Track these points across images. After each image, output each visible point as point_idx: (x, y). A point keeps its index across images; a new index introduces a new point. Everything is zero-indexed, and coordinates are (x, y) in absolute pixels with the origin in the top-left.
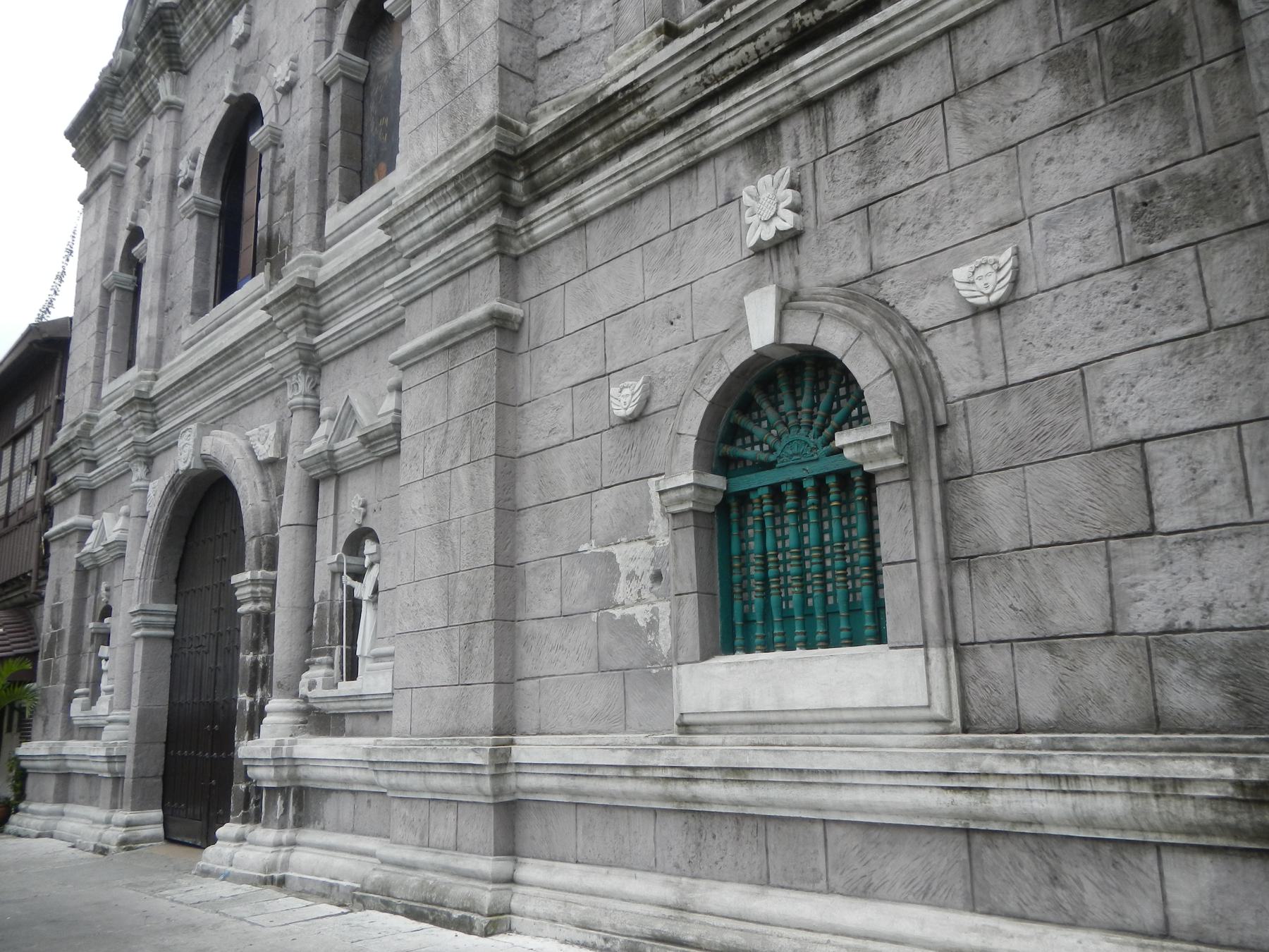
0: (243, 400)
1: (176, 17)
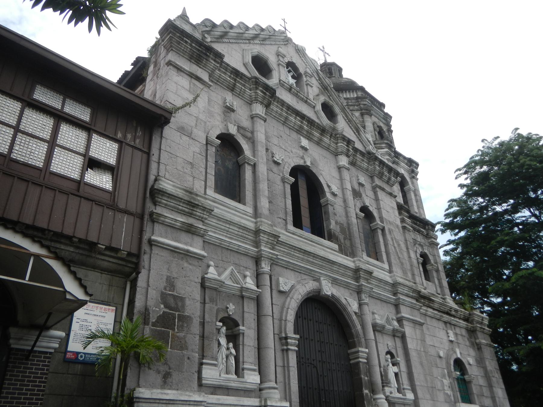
0: (337, 282)
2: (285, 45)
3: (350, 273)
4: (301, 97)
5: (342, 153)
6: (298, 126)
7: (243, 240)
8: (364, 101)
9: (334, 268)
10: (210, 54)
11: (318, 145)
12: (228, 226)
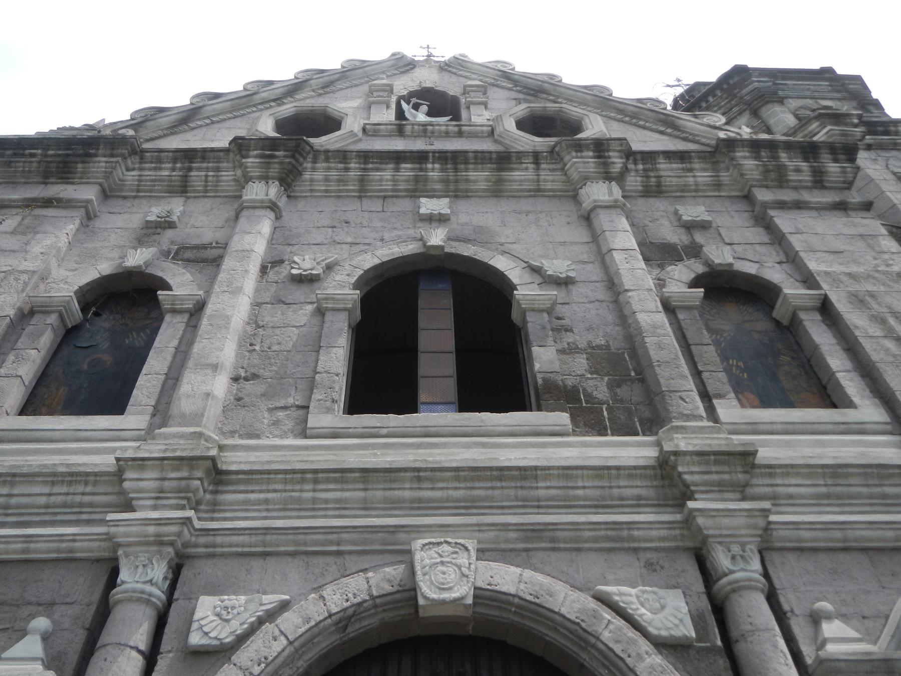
0: (553, 540)
1: (311, 156)
2: (402, 73)
4: (440, 132)
5: (586, 179)
6: (408, 181)
7: (73, 517)
8: (747, 86)
9: (542, 493)
10: (98, 149)
11: (496, 196)
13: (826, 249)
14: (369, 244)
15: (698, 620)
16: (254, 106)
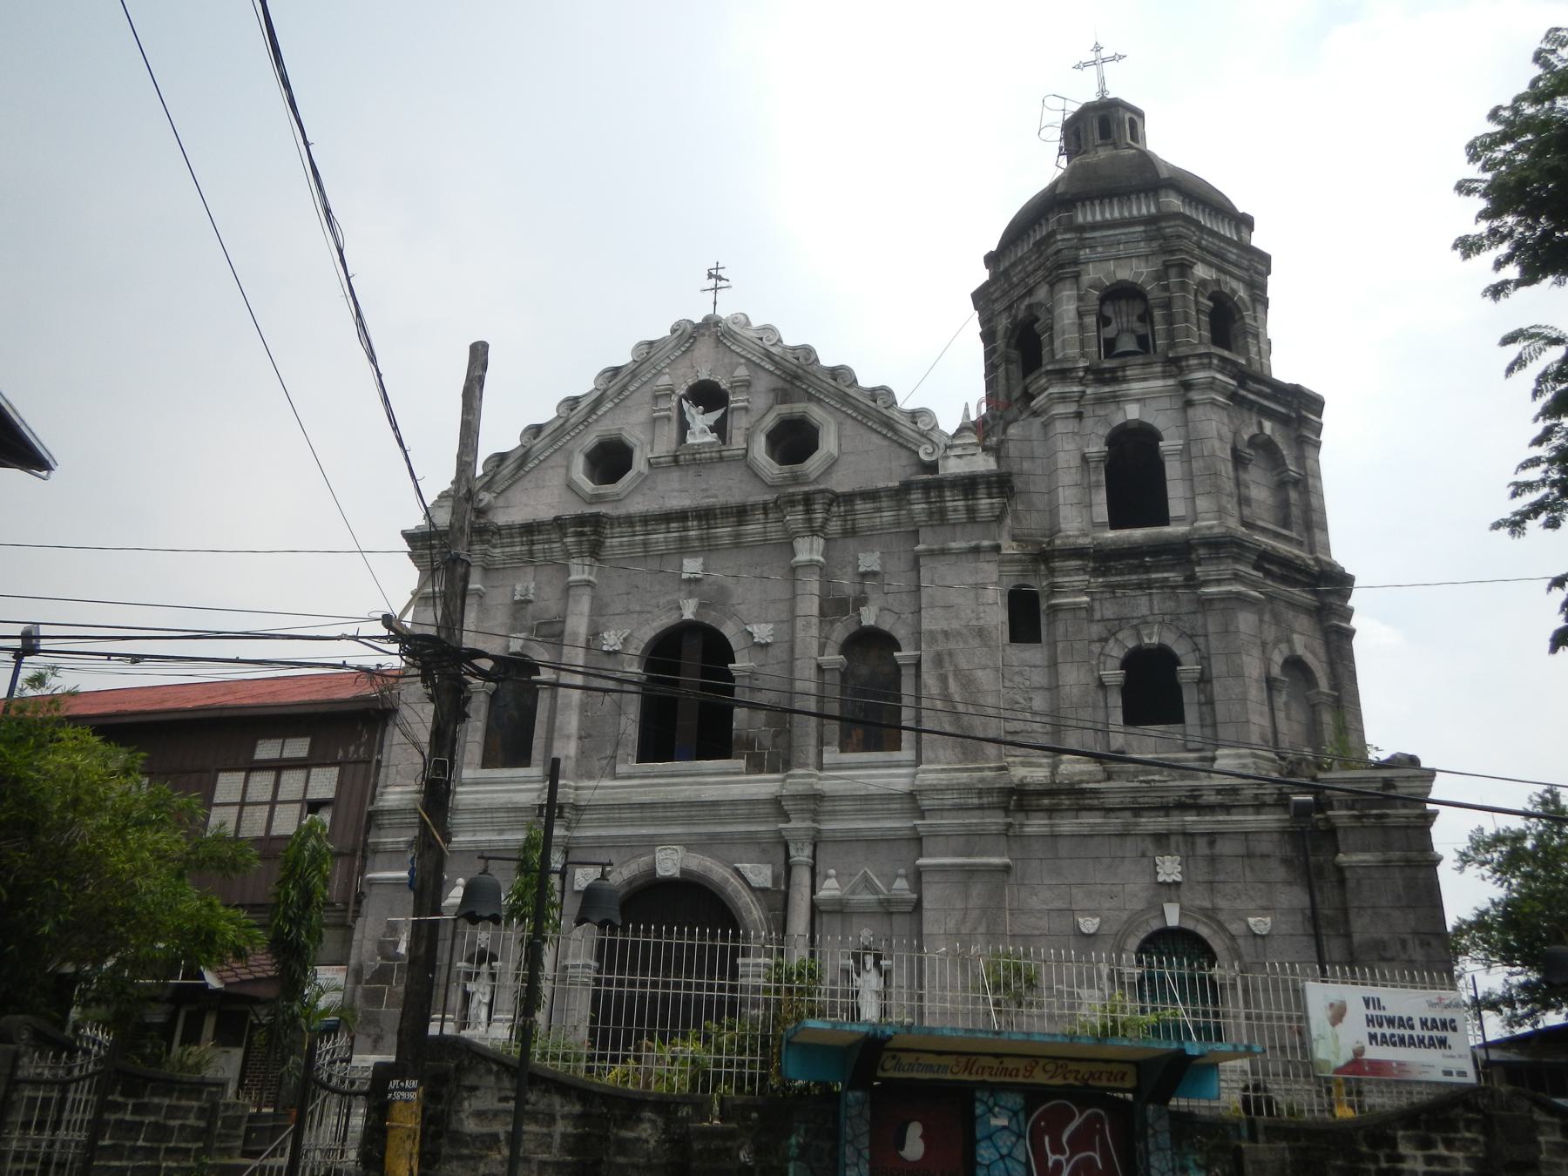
0: (722, 839)
3: (768, 809)
4: (706, 459)
6: (675, 541)
9: (722, 812)
12: (489, 815)
13: (942, 604)
14: (649, 612)
15: (775, 880)
16: (568, 433)
